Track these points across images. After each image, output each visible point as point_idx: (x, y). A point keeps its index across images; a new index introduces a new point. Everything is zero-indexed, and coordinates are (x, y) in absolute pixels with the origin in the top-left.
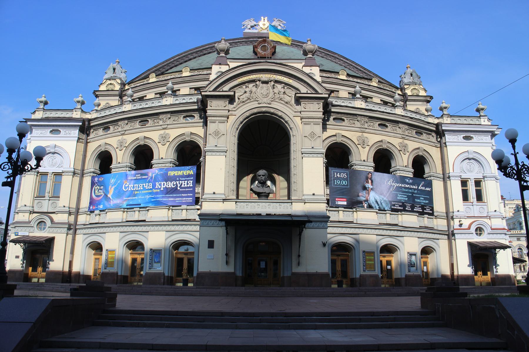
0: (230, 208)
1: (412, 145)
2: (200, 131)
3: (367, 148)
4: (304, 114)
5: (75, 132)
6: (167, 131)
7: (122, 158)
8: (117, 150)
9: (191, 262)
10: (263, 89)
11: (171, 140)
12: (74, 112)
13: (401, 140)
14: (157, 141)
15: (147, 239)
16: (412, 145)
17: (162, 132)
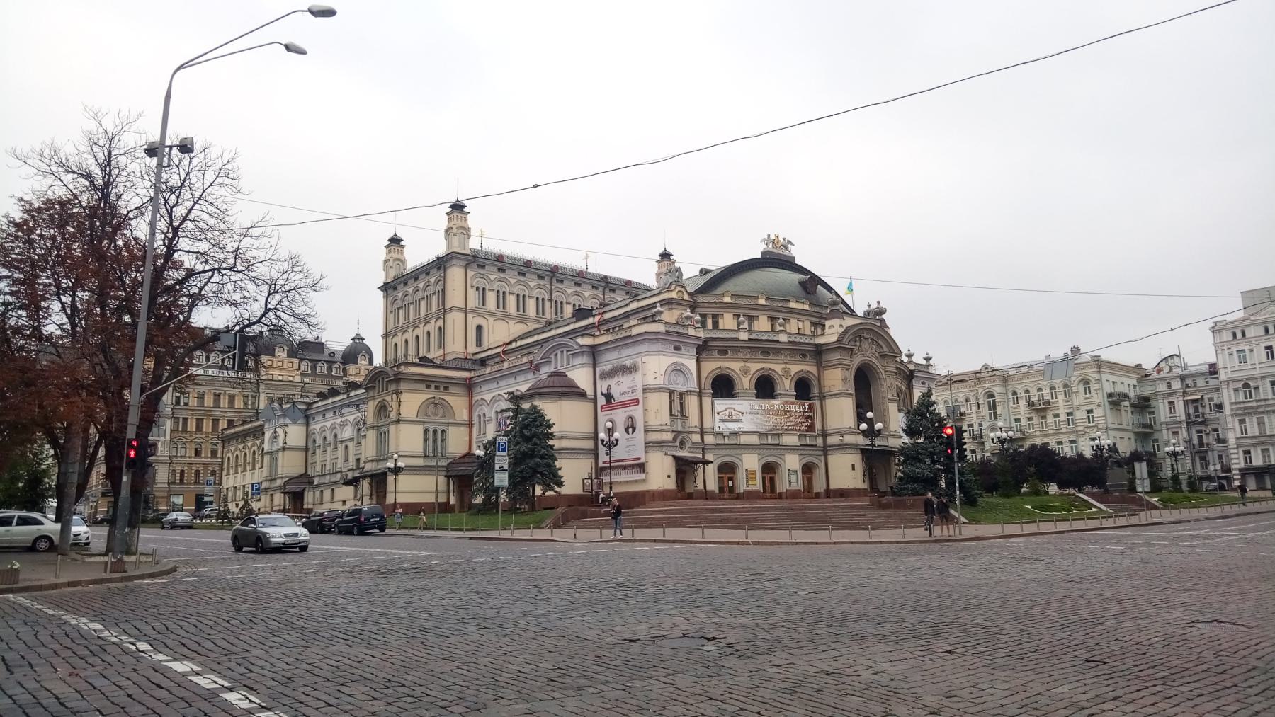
2: (813, 369)
5: (693, 352)
10: (865, 345)
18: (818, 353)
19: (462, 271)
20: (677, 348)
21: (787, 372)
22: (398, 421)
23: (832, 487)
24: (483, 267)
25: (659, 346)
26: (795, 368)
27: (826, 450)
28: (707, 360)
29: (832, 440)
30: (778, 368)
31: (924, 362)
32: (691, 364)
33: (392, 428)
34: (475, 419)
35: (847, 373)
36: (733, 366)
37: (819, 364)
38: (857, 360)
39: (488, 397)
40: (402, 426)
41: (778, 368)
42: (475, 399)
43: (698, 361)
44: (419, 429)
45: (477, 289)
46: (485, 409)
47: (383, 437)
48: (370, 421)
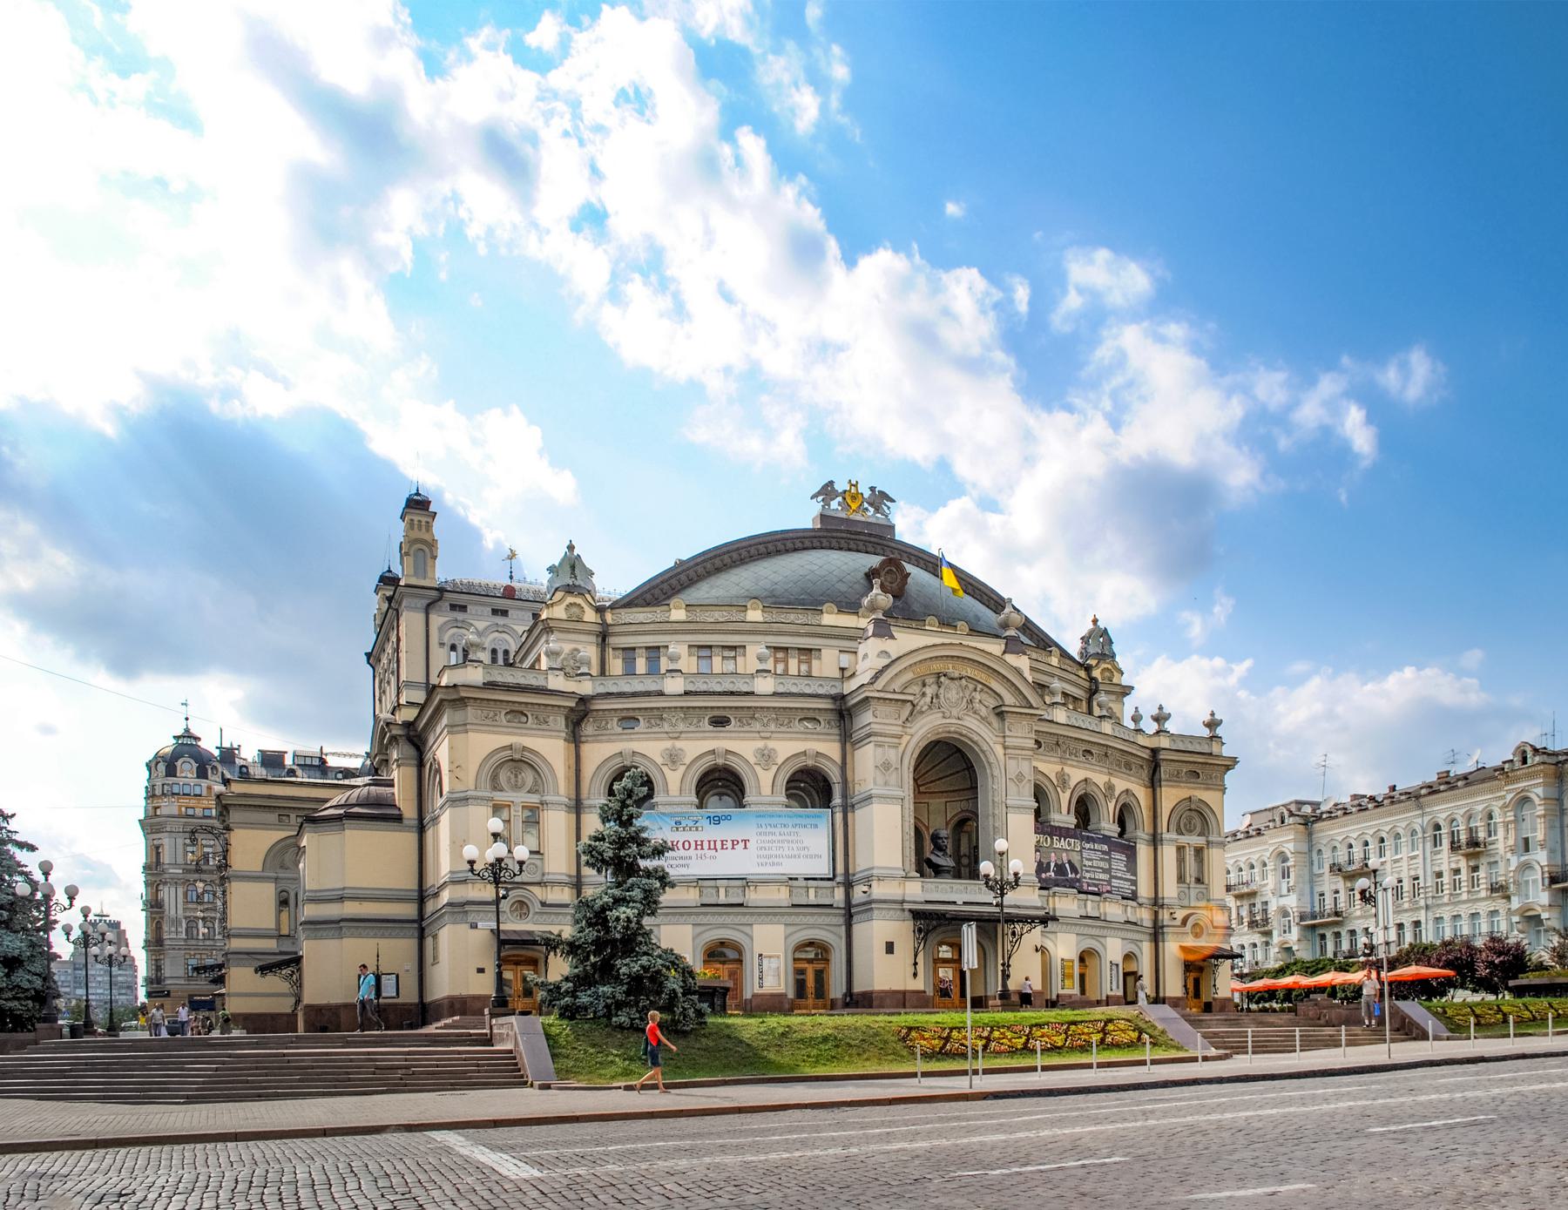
0: (919, 891)
1: (1120, 785)
3: (1068, 792)
4: (1009, 741)
5: (561, 722)
6: (771, 744)
7: (675, 785)
8: (665, 769)
9: (820, 976)
10: (951, 693)
11: (780, 761)
12: (550, 677)
13: (1106, 778)
14: (752, 760)
15: (752, 938)
16: (1120, 785)
17: (760, 744)
19: (422, 616)
20: (517, 713)
21: (766, 757)
23: (857, 989)
24: (463, 608)
25: (471, 713)
28: (596, 738)
31: (1206, 733)
32: (551, 748)
35: (892, 755)
36: (649, 748)
37: (847, 738)
38: (926, 727)
43: (575, 738)
45: (453, 648)
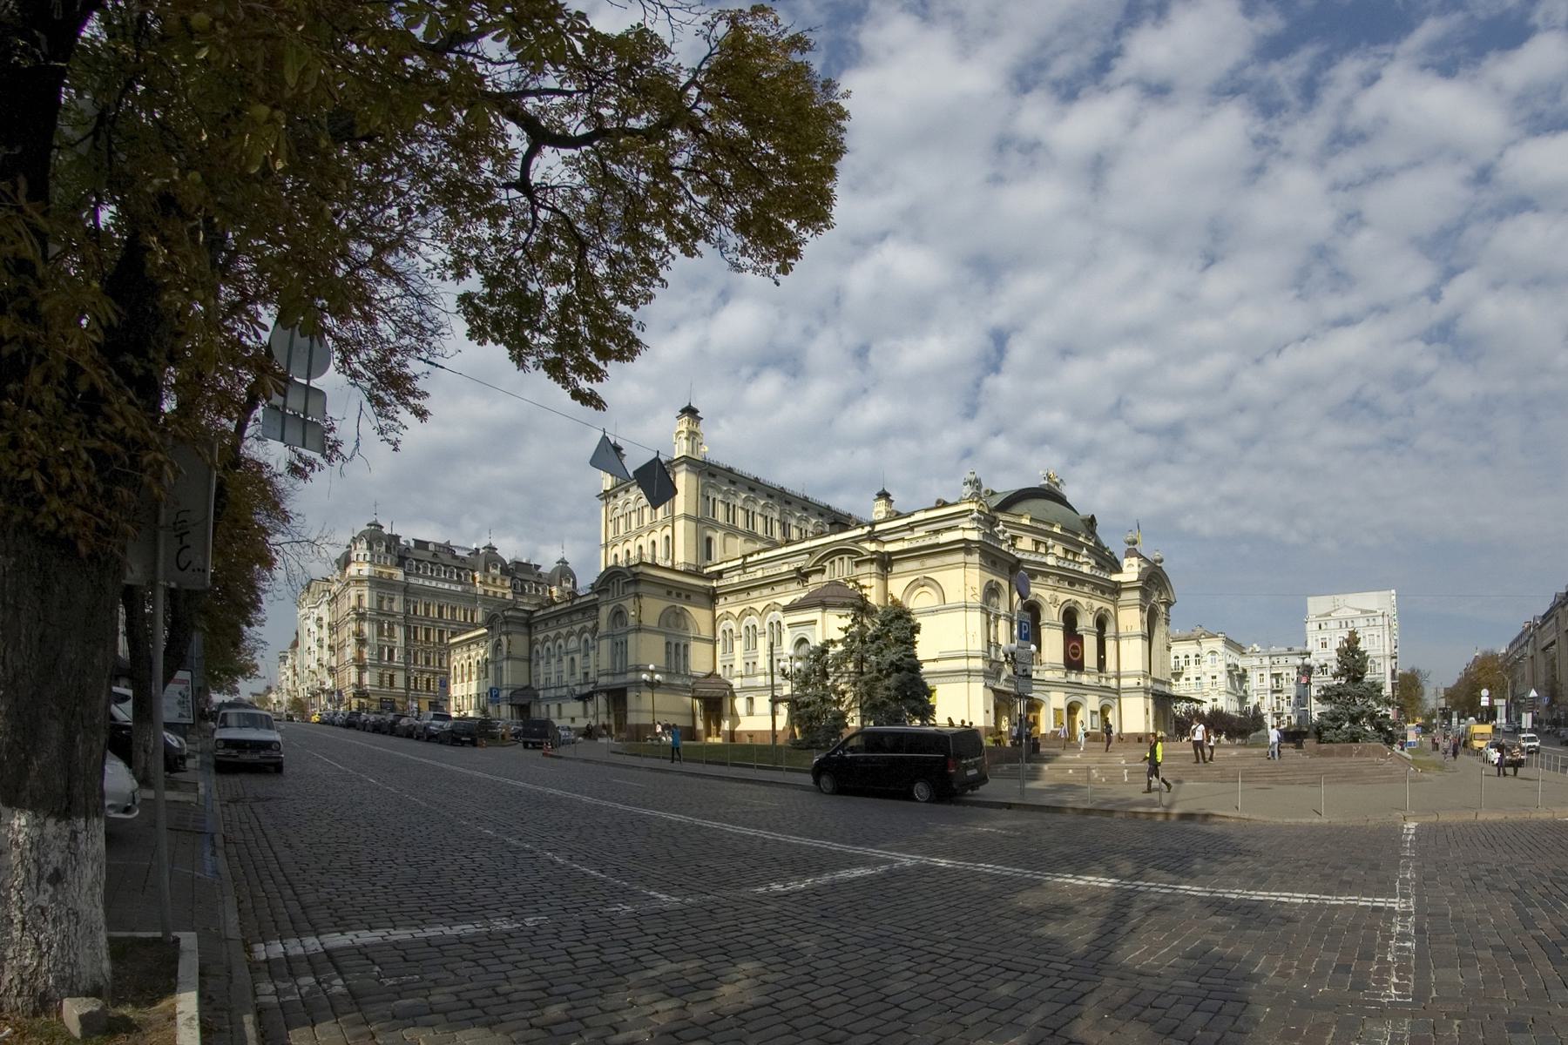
18: (1116, 589)
22: (639, 629)
26: (1097, 604)
27: (1118, 692)
29: (1125, 683)
30: (1083, 601)
33: (631, 638)
34: (719, 634)
39: (736, 611)
40: (642, 635)
41: (1083, 601)
42: (718, 613)
44: (662, 640)
46: (732, 624)
47: (620, 648)
48: (603, 627)
